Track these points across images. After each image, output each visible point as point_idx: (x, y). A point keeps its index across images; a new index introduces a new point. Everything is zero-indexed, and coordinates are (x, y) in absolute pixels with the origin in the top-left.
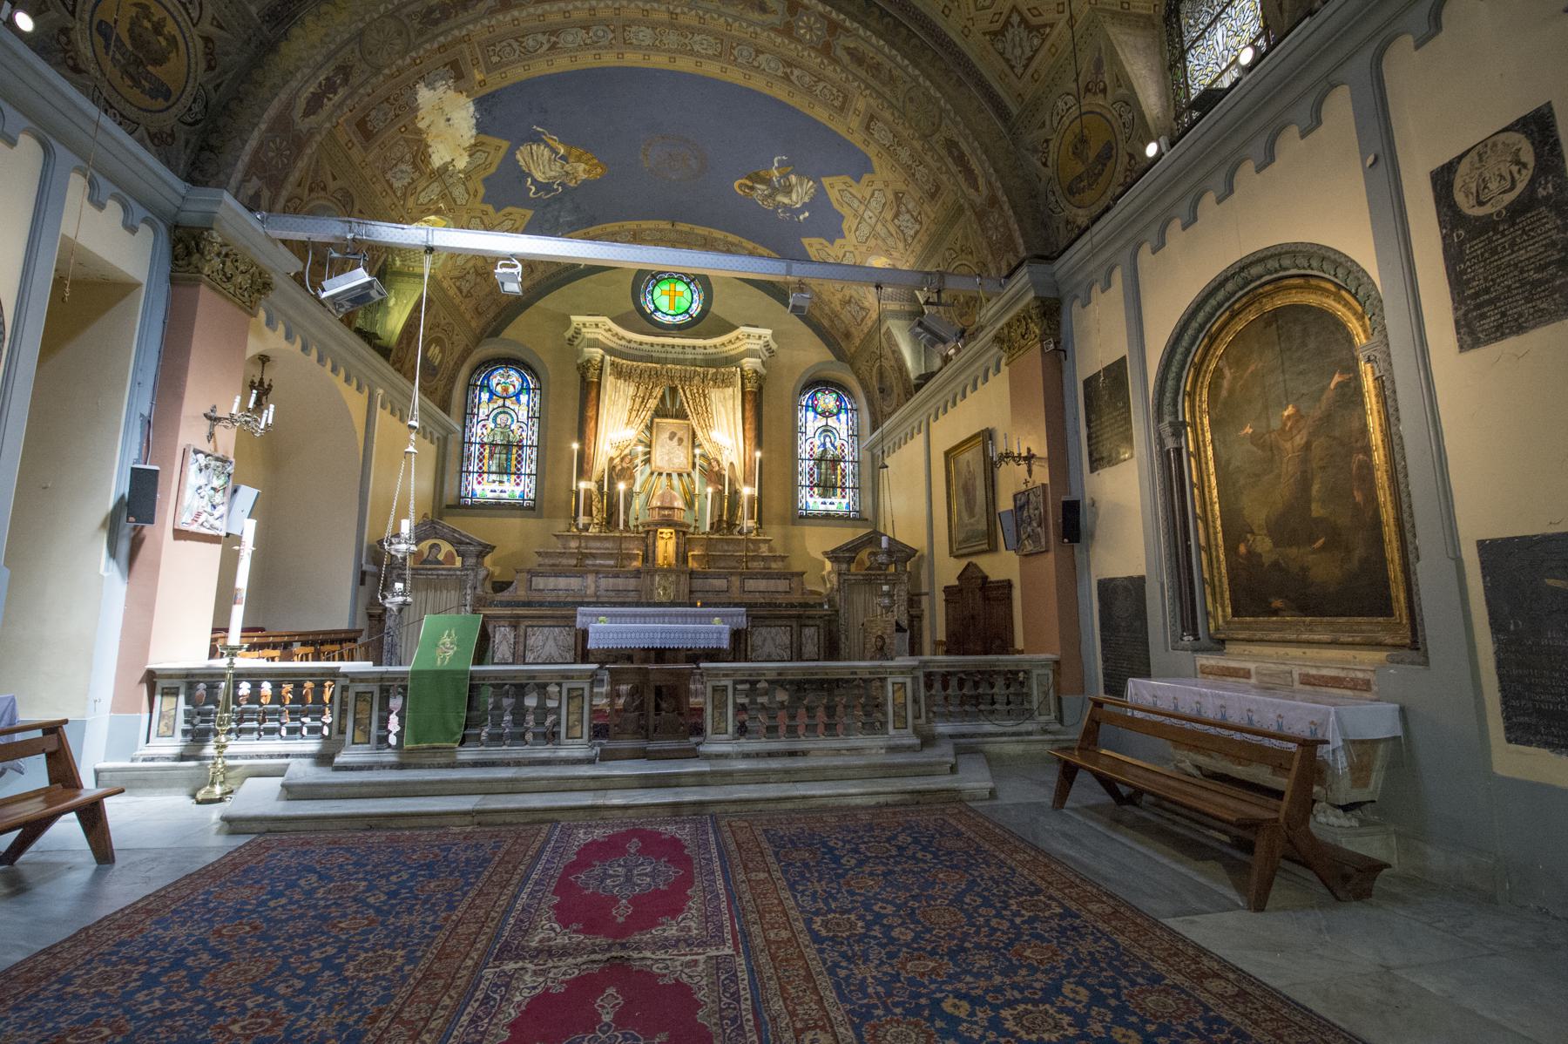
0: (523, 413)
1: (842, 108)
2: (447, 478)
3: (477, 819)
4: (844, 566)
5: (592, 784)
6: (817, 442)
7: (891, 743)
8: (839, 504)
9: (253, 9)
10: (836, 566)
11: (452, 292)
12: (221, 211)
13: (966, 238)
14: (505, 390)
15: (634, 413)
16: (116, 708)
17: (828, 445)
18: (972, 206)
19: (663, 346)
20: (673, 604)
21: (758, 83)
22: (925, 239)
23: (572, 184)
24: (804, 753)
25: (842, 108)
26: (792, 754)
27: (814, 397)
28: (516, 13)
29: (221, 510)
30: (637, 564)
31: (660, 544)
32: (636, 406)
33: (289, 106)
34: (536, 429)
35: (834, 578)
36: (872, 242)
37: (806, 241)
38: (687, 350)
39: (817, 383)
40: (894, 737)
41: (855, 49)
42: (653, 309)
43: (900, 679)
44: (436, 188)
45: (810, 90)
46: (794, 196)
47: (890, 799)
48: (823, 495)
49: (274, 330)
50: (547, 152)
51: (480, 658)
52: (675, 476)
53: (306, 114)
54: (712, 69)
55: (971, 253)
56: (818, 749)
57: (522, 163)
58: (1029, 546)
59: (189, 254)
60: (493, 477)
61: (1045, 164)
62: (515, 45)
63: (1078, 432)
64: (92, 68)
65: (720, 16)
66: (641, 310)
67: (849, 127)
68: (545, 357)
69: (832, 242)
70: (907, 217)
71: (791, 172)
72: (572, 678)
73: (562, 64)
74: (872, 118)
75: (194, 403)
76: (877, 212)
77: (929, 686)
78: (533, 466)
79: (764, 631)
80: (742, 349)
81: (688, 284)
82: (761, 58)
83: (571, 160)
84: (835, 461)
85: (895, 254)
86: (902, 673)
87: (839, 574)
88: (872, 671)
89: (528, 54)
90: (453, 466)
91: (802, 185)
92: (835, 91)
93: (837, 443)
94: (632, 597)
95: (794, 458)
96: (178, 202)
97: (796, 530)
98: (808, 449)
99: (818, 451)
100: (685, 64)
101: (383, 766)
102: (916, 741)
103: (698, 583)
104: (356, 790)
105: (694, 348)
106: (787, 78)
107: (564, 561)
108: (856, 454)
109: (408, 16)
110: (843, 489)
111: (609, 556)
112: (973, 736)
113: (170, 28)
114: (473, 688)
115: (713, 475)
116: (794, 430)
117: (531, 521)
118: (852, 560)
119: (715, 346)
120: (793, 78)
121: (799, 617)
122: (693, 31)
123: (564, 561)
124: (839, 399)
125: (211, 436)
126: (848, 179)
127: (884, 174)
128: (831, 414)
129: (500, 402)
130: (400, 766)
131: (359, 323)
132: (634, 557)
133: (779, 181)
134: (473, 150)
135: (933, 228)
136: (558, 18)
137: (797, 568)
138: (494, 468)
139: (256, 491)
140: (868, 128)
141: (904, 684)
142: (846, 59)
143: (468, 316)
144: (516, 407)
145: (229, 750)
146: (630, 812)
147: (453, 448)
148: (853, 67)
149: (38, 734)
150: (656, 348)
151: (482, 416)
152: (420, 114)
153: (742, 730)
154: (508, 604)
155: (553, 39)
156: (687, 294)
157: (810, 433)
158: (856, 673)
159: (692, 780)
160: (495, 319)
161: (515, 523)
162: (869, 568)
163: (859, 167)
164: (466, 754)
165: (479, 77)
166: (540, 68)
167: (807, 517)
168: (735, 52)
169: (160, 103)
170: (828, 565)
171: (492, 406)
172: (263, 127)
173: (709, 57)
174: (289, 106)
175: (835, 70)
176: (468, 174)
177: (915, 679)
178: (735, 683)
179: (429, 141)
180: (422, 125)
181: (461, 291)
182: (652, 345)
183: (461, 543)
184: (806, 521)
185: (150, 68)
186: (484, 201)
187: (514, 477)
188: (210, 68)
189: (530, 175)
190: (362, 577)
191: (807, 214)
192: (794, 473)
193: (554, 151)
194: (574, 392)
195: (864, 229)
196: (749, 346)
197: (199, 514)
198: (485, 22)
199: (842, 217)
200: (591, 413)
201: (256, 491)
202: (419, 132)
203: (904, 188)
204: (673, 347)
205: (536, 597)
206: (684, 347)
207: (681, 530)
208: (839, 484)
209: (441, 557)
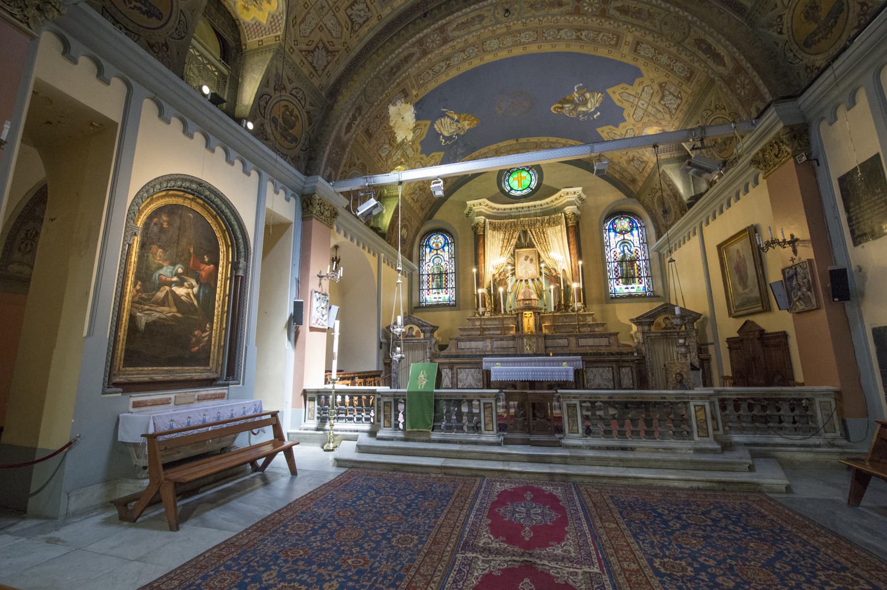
0: (446, 256)
1: (617, 44)
2: (414, 294)
3: (443, 471)
4: (646, 328)
5: (501, 457)
6: (618, 250)
7: (697, 446)
8: (637, 288)
9: (323, 94)
10: (640, 328)
11: (410, 201)
12: (318, 185)
13: (719, 99)
14: (437, 245)
15: (504, 248)
16: (293, 407)
17: (626, 251)
18: (721, 77)
19: (517, 208)
20: (535, 355)
21: (561, 47)
22: (685, 108)
23: (462, 133)
24: (632, 449)
25: (617, 44)
26: (623, 449)
27: (613, 223)
28: (430, 56)
29: (326, 317)
30: (513, 332)
31: (525, 320)
32: (505, 244)
33: (339, 131)
34: (453, 263)
35: (640, 336)
36: (646, 119)
37: (599, 130)
38: (531, 209)
39: (615, 214)
40: (699, 442)
41: (622, 6)
42: (509, 188)
43: (700, 403)
44: (400, 152)
45: (594, 40)
46: (589, 106)
47: (701, 485)
48: (626, 283)
49: (340, 233)
50: (448, 120)
51: (438, 386)
52: (530, 281)
53: (346, 133)
54: (533, 49)
55: (724, 108)
56: (642, 447)
57: (437, 129)
58: (800, 306)
59: (308, 206)
60: (435, 291)
61: (781, 33)
62: (430, 72)
63: (837, 218)
64: (272, 138)
65: (535, 18)
66: (503, 191)
67: (624, 55)
68: (456, 227)
69: (617, 126)
70: (671, 97)
71: (586, 92)
72: (485, 397)
73: (453, 73)
74: (638, 43)
75: (314, 271)
76: (647, 100)
77: (723, 408)
78: (453, 283)
79: (594, 370)
80: (564, 202)
81: (528, 171)
82: (562, 32)
83: (461, 121)
84: (632, 261)
85: (663, 123)
86: (702, 399)
87: (643, 333)
88: (677, 397)
89: (436, 74)
90: (415, 288)
91: (593, 97)
92: (611, 35)
93: (633, 249)
94: (512, 351)
95: (604, 262)
96: (302, 184)
97: (610, 307)
98: (613, 256)
99: (619, 256)
100: (518, 51)
101: (398, 439)
102: (718, 447)
103: (550, 342)
104: (387, 450)
105: (535, 206)
106: (579, 38)
107: (474, 333)
108: (647, 255)
109: (384, 75)
110: (640, 278)
111: (498, 329)
112: (765, 445)
113: (296, 112)
115: (553, 278)
116: (602, 245)
117: (455, 312)
118: (652, 323)
119: (547, 203)
120: (583, 37)
121: (617, 361)
122: (519, 32)
123: (474, 333)
124: (631, 221)
125: (320, 284)
126: (624, 85)
127: (651, 75)
128: (627, 232)
130: (405, 440)
131: (372, 224)
132: (511, 329)
133: (578, 99)
134: (414, 130)
135: (690, 100)
136: (449, 51)
137: (612, 330)
138: (434, 287)
139: (337, 308)
140: (636, 50)
141: (703, 407)
142: (617, 14)
143: (417, 212)
144: (442, 254)
145: (335, 427)
146: (525, 476)
147: (415, 278)
148: (622, 17)
149: (269, 416)
150: (513, 210)
152: (391, 119)
153: (588, 432)
154: (447, 357)
155: (448, 62)
156: (528, 177)
157: (613, 245)
158: (665, 398)
159: (558, 460)
160: (430, 210)
161: (447, 314)
162: (665, 328)
163: (630, 75)
164: (435, 436)
165: (414, 93)
166: (443, 79)
167: (616, 297)
168: (546, 35)
169: (294, 144)
170: (635, 328)
172: (330, 144)
173: (529, 43)
174: (339, 131)
175: (610, 24)
176: (413, 141)
177: (712, 403)
178: (581, 402)
179: (396, 131)
180: (392, 124)
181: (413, 200)
182: (511, 209)
183: (423, 326)
184: (616, 300)
185: (290, 131)
186: (422, 153)
187: (444, 290)
188: (310, 124)
189: (441, 134)
190: (381, 345)
191: (599, 114)
192: (605, 272)
193: (452, 119)
194: (471, 242)
195: (640, 113)
196: (569, 200)
197: (318, 320)
198: (416, 65)
199: (623, 109)
200: (481, 251)
201: (337, 308)
202: (391, 127)
203: (666, 79)
204: (523, 208)
205: (461, 353)
206: (529, 207)
207: (537, 311)
208: (636, 275)
209: (414, 334)
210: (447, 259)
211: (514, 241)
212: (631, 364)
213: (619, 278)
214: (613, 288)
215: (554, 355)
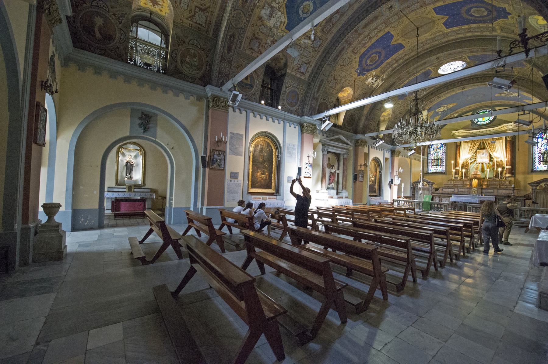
0: (441, 152)
2: (425, 167)
4: (534, 188)
6: (543, 148)
15: (470, 150)
30: (468, 186)
32: (471, 148)
34: (445, 155)
51: (432, 200)
78: (445, 163)
80: (506, 129)
90: (425, 165)
97: (530, 176)
98: (538, 151)
99: (543, 151)
107: (450, 185)
111: (461, 185)
114: (431, 204)
117: (444, 176)
118: (537, 186)
123: (450, 185)
129: (436, 150)
132: (468, 185)
138: (435, 165)
144: (440, 151)
147: (426, 162)
151: (432, 154)
154: (437, 193)
161: (440, 176)
162: (545, 188)
171: (434, 151)
187: (440, 166)
200: (458, 152)
205: (445, 192)
207: (478, 179)
210: (441, 153)
211: (476, 147)
212: (522, 201)
213: (542, 161)
214: (536, 166)
215: (485, 195)
